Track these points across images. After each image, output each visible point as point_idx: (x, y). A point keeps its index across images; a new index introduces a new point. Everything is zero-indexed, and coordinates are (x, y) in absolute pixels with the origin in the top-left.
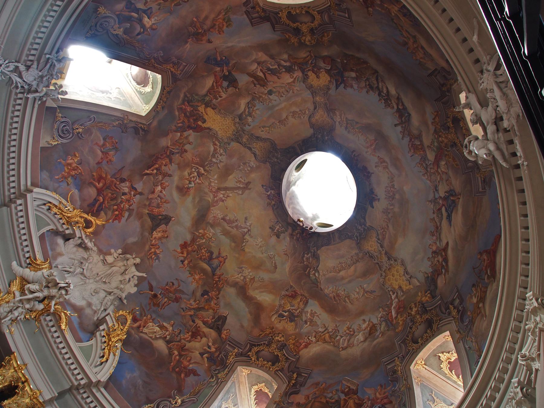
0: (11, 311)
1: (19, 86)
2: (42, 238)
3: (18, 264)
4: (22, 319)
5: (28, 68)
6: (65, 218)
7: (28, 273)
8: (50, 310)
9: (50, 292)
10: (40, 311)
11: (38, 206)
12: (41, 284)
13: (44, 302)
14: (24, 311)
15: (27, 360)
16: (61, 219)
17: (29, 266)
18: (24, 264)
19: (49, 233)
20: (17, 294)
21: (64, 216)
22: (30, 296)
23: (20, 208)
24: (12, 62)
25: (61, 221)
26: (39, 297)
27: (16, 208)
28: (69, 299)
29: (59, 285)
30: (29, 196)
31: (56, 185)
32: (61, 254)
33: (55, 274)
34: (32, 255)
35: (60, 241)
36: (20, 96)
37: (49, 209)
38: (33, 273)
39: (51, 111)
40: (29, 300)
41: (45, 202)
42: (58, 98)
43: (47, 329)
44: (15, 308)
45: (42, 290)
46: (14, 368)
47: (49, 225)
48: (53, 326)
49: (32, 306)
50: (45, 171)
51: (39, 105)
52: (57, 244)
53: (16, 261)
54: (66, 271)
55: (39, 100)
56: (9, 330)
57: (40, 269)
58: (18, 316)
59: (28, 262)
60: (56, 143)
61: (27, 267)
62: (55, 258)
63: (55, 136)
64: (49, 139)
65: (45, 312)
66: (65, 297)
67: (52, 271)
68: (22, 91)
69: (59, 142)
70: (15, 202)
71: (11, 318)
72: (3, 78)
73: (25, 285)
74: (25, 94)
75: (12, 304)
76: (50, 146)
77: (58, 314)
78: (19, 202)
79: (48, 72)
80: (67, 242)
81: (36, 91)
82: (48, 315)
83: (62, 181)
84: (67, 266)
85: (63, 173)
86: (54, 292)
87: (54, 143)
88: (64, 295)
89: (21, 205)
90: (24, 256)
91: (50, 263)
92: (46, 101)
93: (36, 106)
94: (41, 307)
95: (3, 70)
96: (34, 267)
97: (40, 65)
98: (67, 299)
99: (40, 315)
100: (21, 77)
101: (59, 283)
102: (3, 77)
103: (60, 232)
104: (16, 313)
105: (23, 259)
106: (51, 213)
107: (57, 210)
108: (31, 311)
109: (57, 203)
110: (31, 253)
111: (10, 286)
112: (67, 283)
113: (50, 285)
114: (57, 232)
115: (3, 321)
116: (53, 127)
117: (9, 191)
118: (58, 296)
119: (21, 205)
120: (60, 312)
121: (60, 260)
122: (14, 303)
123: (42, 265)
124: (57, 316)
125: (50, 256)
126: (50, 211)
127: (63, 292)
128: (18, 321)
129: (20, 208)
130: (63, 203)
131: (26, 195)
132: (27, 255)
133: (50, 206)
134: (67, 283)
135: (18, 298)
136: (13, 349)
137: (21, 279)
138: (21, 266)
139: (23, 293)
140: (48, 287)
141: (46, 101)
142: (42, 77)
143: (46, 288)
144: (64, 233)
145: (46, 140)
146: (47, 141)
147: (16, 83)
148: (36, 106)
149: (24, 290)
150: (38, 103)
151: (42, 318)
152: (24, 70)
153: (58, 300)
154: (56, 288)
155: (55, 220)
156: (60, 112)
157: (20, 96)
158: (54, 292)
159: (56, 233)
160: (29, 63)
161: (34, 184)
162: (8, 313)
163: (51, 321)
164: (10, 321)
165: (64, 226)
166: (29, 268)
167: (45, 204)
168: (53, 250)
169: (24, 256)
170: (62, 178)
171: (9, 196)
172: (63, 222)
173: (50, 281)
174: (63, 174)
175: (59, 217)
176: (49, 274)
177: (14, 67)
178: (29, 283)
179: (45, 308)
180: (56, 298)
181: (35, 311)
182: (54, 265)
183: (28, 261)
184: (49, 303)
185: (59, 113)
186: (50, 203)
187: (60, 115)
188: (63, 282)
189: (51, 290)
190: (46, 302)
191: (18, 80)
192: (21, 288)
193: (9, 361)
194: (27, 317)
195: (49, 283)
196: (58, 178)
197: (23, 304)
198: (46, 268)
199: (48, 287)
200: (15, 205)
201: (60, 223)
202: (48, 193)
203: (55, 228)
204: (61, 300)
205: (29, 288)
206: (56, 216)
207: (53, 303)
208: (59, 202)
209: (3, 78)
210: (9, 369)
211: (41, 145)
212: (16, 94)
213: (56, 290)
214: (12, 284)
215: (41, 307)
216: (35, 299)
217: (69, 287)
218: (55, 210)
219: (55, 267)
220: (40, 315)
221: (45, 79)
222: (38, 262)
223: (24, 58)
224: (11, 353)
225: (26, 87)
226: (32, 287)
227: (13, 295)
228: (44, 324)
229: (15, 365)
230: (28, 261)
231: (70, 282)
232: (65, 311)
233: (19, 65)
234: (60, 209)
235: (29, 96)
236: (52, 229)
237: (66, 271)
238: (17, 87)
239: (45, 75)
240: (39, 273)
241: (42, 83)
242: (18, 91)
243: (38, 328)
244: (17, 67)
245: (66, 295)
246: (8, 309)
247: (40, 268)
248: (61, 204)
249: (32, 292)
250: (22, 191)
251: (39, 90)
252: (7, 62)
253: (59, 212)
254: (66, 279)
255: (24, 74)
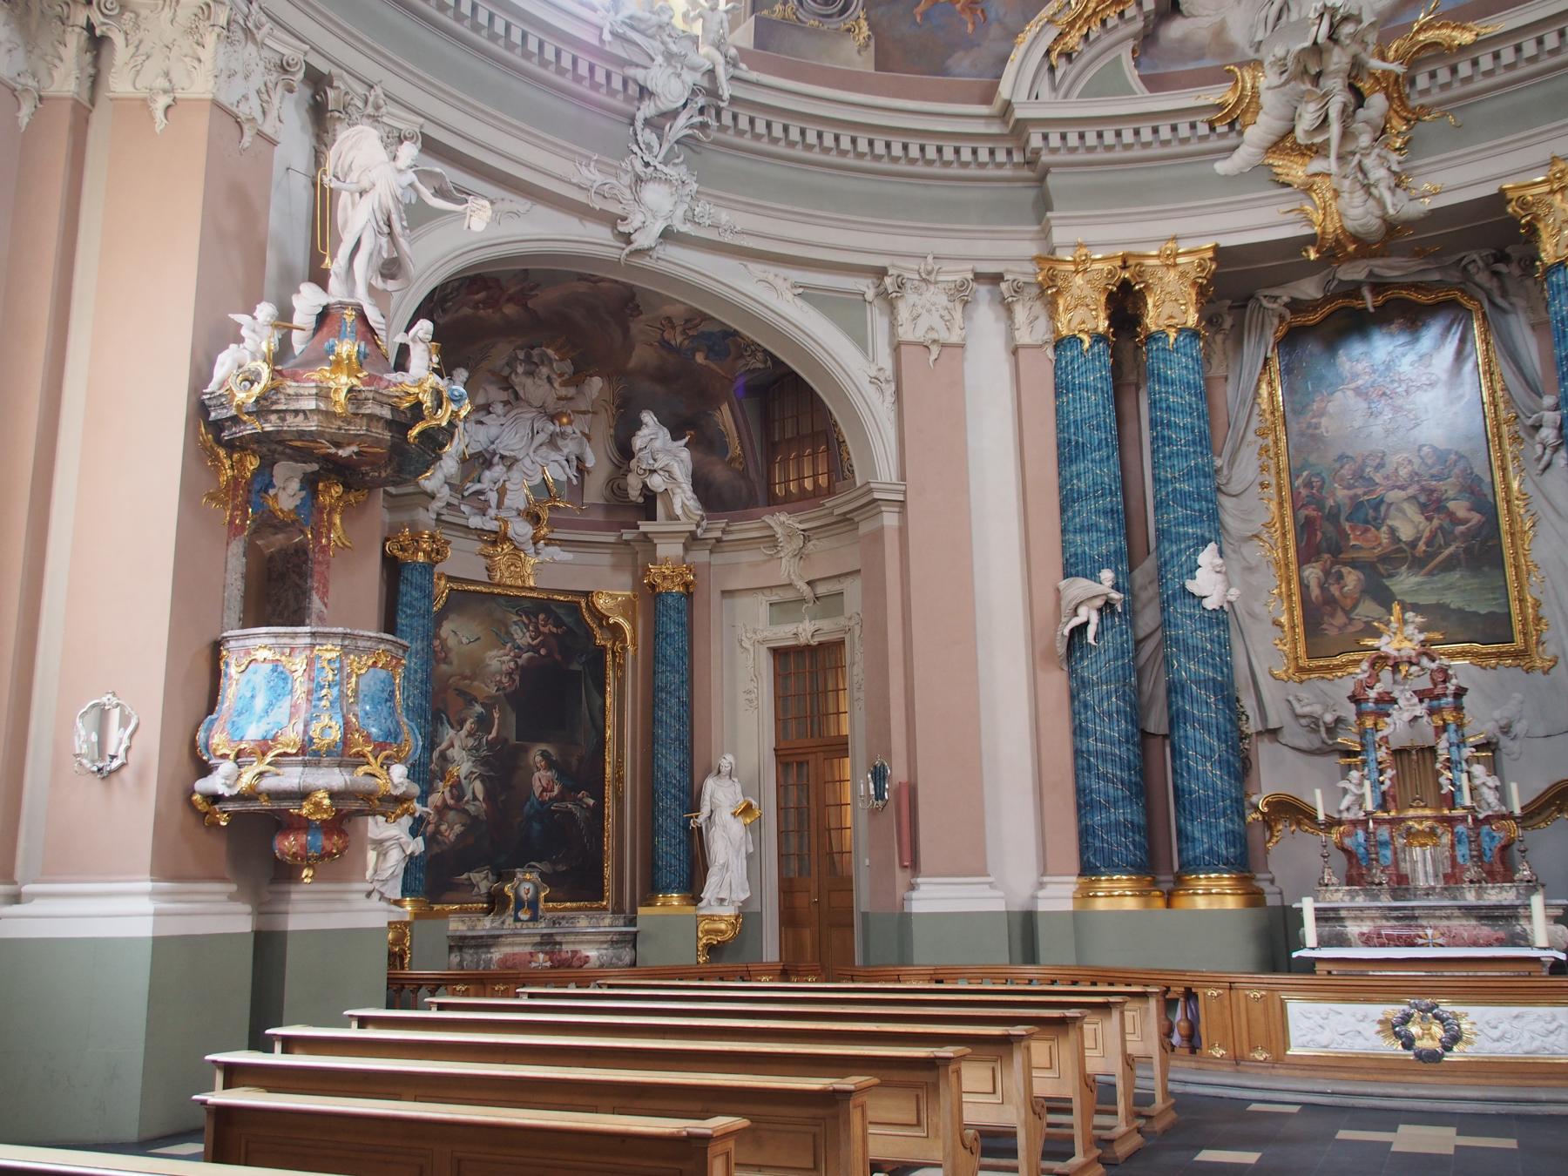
0: (1367, 188)
1: (700, 119)
2: (1154, 83)
3: (1225, 158)
4: (1401, 158)
5: (644, 92)
6: (1103, 9)
7: (1258, 132)
8: (1398, 76)
9: (1338, 72)
10: (1391, 106)
11: (1054, 88)
12: (1302, 97)
13: (1366, 93)
14: (1376, 151)
15: (1542, 153)
16: (1104, 22)
17: (1238, 127)
18: (1231, 140)
19: (1144, 60)
20: (1317, 165)
21: (1095, 13)
22: (1335, 130)
23: (1055, 141)
24: (636, 134)
25: (1110, 24)
26: (1345, 105)
27: (1054, 151)
28: (1379, 14)
29: (1320, 40)
30: (1019, 113)
31: (995, 31)
32: (1220, 30)
33: (1279, 51)
34: (1206, 117)
35: (1176, 29)
36: (727, 119)
37: (1068, 56)
38: (1261, 118)
39: (765, 33)
40: (1346, 134)
41: (1046, 67)
42: (727, 12)
43: (1457, 90)
44: (1360, 176)
45: (1325, 95)
46: (1553, 192)
47: (1118, 59)
48: (1454, 70)
49: (1369, 129)
50: (950, 62)
51: (751, 68)
52: (1183, 41)
53: (1216, 160)
54: (1279, 18)
55: (735, 66)
56: (1424, 197)
57: (1256, 94)
58: (1389, 169)
59: (1226, 129)
60: (864, 24)
61: (1241, 133)
62: (1228, 49)
63: (843, 27)
64: (850, 46)
65: (1399, 92)
66: (1365, 24)
67: (1269, 60)
68: (713, 112)
69: (861, 14)
70: (1037, 152)
71: (1389, 188)
72: (681, 159)
73: (1295, 142)
74: (722, 105)
75: (1347, 183)
76: (872, 43)
77: (1418, 52)
78: (1036, 141)
79: (652, 37)
80: (1183, 7)
81: (711, 73)
82: (1412, 82)
83: (983, 11)
84: (1263, 14)
85: (958, 6)
86: (1338, 60)
87: (865, 31)
88: (1360, 27)
89: (1045, 137)
90: (1203, 138)
91: (1240, 65)
92: (738, 48)
93: (754, 76)
94: (1377, 103)
95: (660, 158)
96: (1244, 112)
97: (635, 59)
98: (1373, 19)
99: (1403, 104)
100: (674, 114)
101: (1315, 43)
102: (677, 161)
103: (1145, 27)
104: (1378, 173)
105: (1214, 143)
106: (1080, 53)
107: (1072, 33)
108: (1384, 131)
109: (1053, 33)
110: (1198, 118)
111: (1289, 185)
112: (1322, 15)
113: (1314, 70)
114: (1146, 37)
115: (1391, 211)
116: (813, 31)
117: (1000, 165)
118: (1355, 48)
119: (1045, 137)
120: (1413, 46)
121: (1238, 34)
122: (1345, 177)
123: (1243, 88)
124: (1424, 54)
125: (1217, 63)
126: (1074, 55)
127: (1348, 29)
128: (1403, 170)
129: (1055, 141)
130: (1055, 14)
131: (1018, 121)
132: (1203, 129)
133: (1060, 55)
134: (1322, 15)
135: (1331, 164)
136: (1490, 190)
137: (1274, 152)
138: (1235, 148)
139: (1319, 151)
140: (1319, 74)
141: (738, 48)
142: (669, 56)
143: (1322, 81)
144: (1152, 17)
145: (855, 53)
146: (859, 52)
147: (691, 126)
148: (754, 76)
149: (1308, 147)
150: (744, 71)
151: (1416, 101)
152: (652, 104)
153: (1371, 48)
154: (1329, 51)
155: (1107, 40)
156: (770, 7)
157: (727, 119)
158: (1338, 60)
159: (1147, 40)
160: (633, 90)
161: (988, 96)
162: (1371, 194)
163: (1433, 75)
164: (1399, 191)
165: (1128, 14)
166: (1245, 126)
167: (1052, 69)
168: (1200, 54)
169: (1203, 138)
170: (973, 12)
171: (1017, 166)
172: (1116, 17)
173: (1301, 67)
174: (963, 9)
175: (1096, 28)
176: (1276, 69)
177: (648, 131)
178: (1292, 130)
179: (1386, 89)
180: (1364, 56)
181: (1388, 120)
182: (1251, 54)
183: (1222, 128)
184: (1372, 75)
185: (774, 12)
186: (1048, 52)
187: (778, 7)
188: (1316, 28)
189: (1332, 67)
190: (1365, 85)
191: (682, 120)
192: (1303, 155)
193: (1523, 204)
194: (1398, 145)
195: (1305, 71)
196: (974, 23)
197: (1353, 153)
198: (1254, 78)
199: (1319, 74)
200: (1043, 152)
201: (1115, 27)
202: (1016, 55)
203: (1131, 43)
204: (1372, 38)
205: (1306, 132)
206: (1092, 37)
207: (1376, 64)
208: (1048, 26)
209: (681, 159)
210: (1550, 206)
211: (873, 71)
212: (723, 129)
213: (1337, 51)
214: (1283, 178)
215: (1377, 103)
216: (1347, 115)
217: (1333, 10)
218: (1073, 40)
219: (1257, 50)
220: (1403, 104)
221: (674, 48)
222: (1232, 99)
223: (618, 102)
224: (1501, 198)
225: (701, 101)
226: (1308, 117)
227: (1317, 179)
228: (1437, 96)
229: (1546, 188)
230: (1222, 128)
231: (1319, 5)
232: (1416, 27)
233: (640, 116)
234: (1071, 24)
235: (726, 96)
236: (1134, 52)
237: (1279, 18)
238: (704, 126)
239: (662, 48)
240: (1267, 99)
241: (685, 56)
242: (713, 123)
243: (1444, 115)
244: (647, 122)
245: (1358, 20)
246: (1359, 195)
247: (1252, 97)
248: (1056, 18)
249: (1324, 122)
250: (1006, 131)
251: (708, 65)
252: (635, 148)
253: (1080, 28)
254: (1307, 18)
255: (666, 104)
